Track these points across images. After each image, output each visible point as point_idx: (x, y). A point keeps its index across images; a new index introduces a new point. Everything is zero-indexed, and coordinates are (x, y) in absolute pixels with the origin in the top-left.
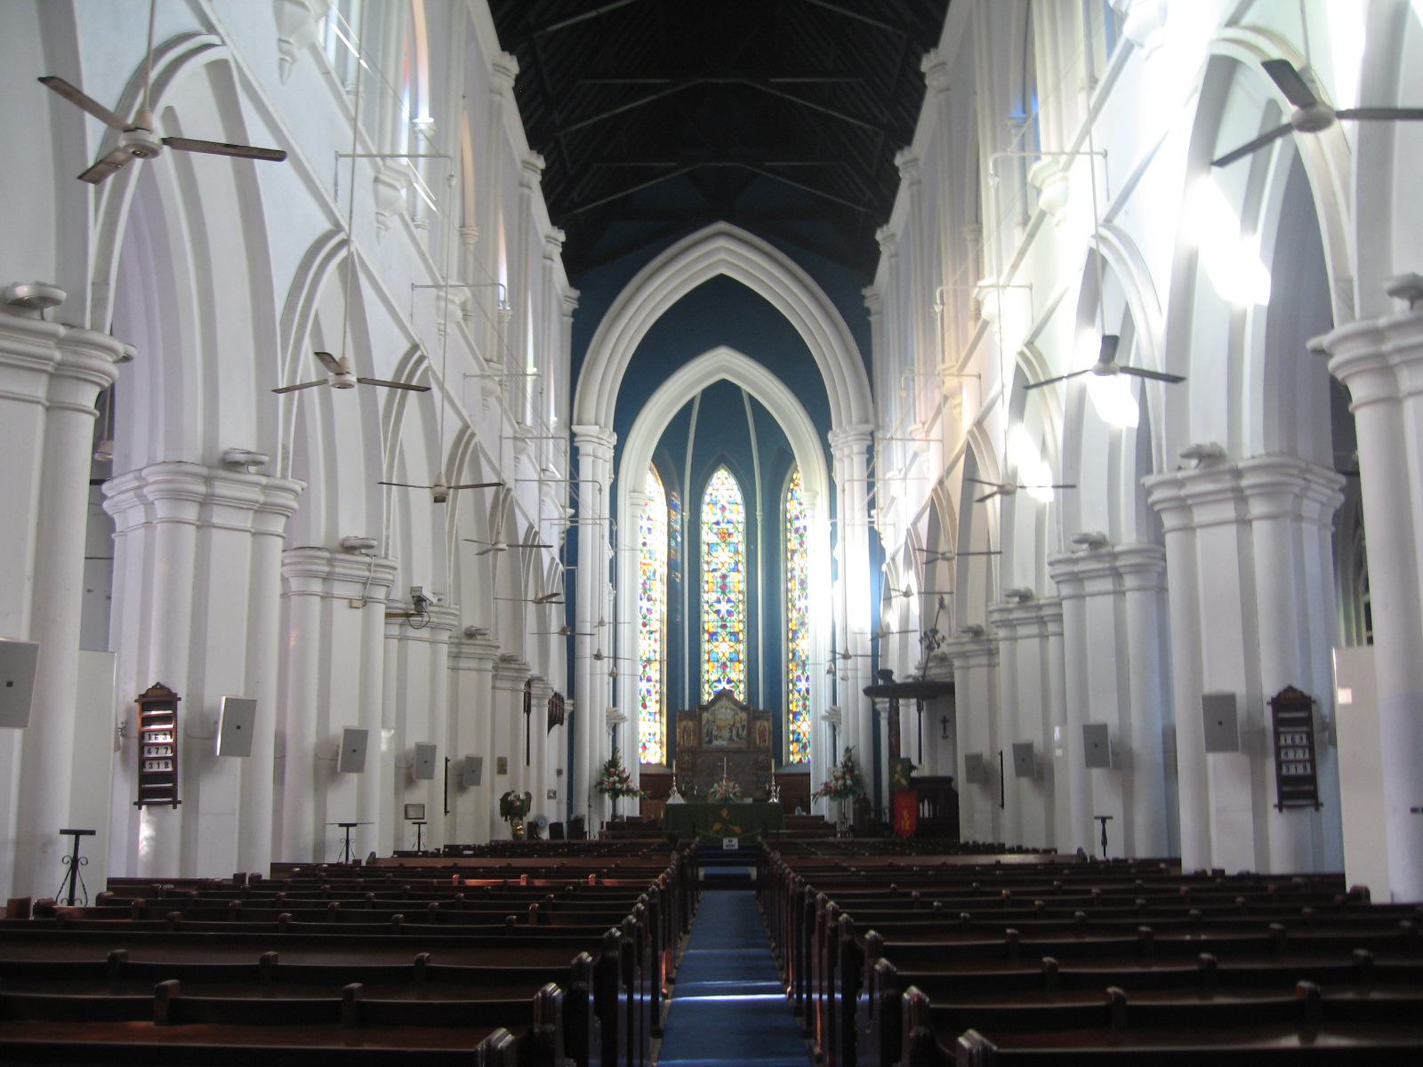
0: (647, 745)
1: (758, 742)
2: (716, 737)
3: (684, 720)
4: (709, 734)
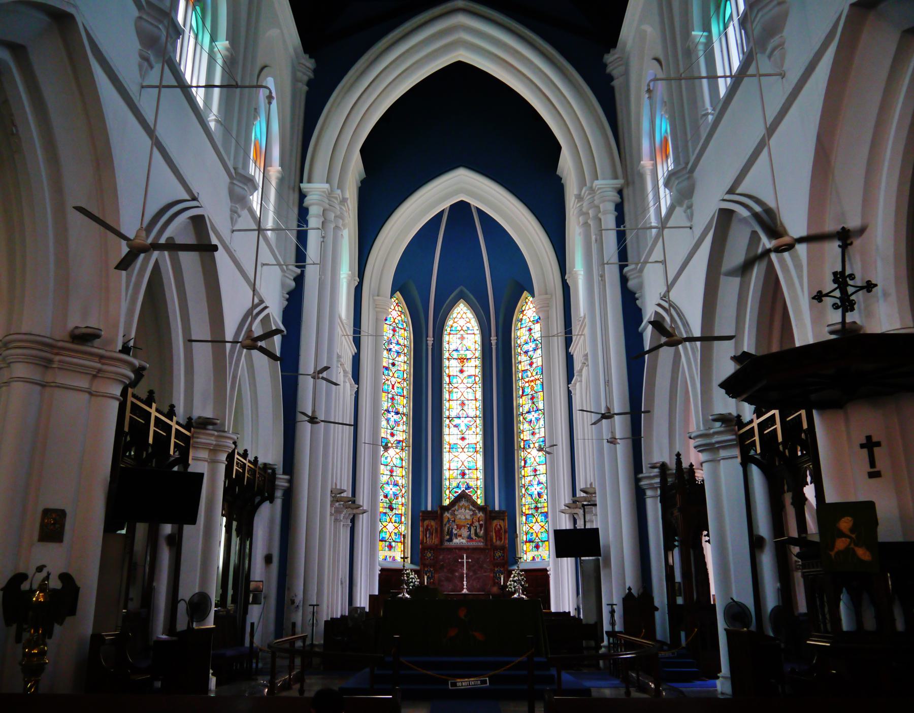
0: (393, 544)
1: (494, 540)
2: (457, 536)
3: (427, 520)
4: (450, 533)
